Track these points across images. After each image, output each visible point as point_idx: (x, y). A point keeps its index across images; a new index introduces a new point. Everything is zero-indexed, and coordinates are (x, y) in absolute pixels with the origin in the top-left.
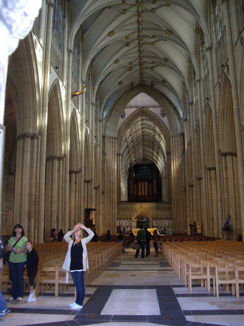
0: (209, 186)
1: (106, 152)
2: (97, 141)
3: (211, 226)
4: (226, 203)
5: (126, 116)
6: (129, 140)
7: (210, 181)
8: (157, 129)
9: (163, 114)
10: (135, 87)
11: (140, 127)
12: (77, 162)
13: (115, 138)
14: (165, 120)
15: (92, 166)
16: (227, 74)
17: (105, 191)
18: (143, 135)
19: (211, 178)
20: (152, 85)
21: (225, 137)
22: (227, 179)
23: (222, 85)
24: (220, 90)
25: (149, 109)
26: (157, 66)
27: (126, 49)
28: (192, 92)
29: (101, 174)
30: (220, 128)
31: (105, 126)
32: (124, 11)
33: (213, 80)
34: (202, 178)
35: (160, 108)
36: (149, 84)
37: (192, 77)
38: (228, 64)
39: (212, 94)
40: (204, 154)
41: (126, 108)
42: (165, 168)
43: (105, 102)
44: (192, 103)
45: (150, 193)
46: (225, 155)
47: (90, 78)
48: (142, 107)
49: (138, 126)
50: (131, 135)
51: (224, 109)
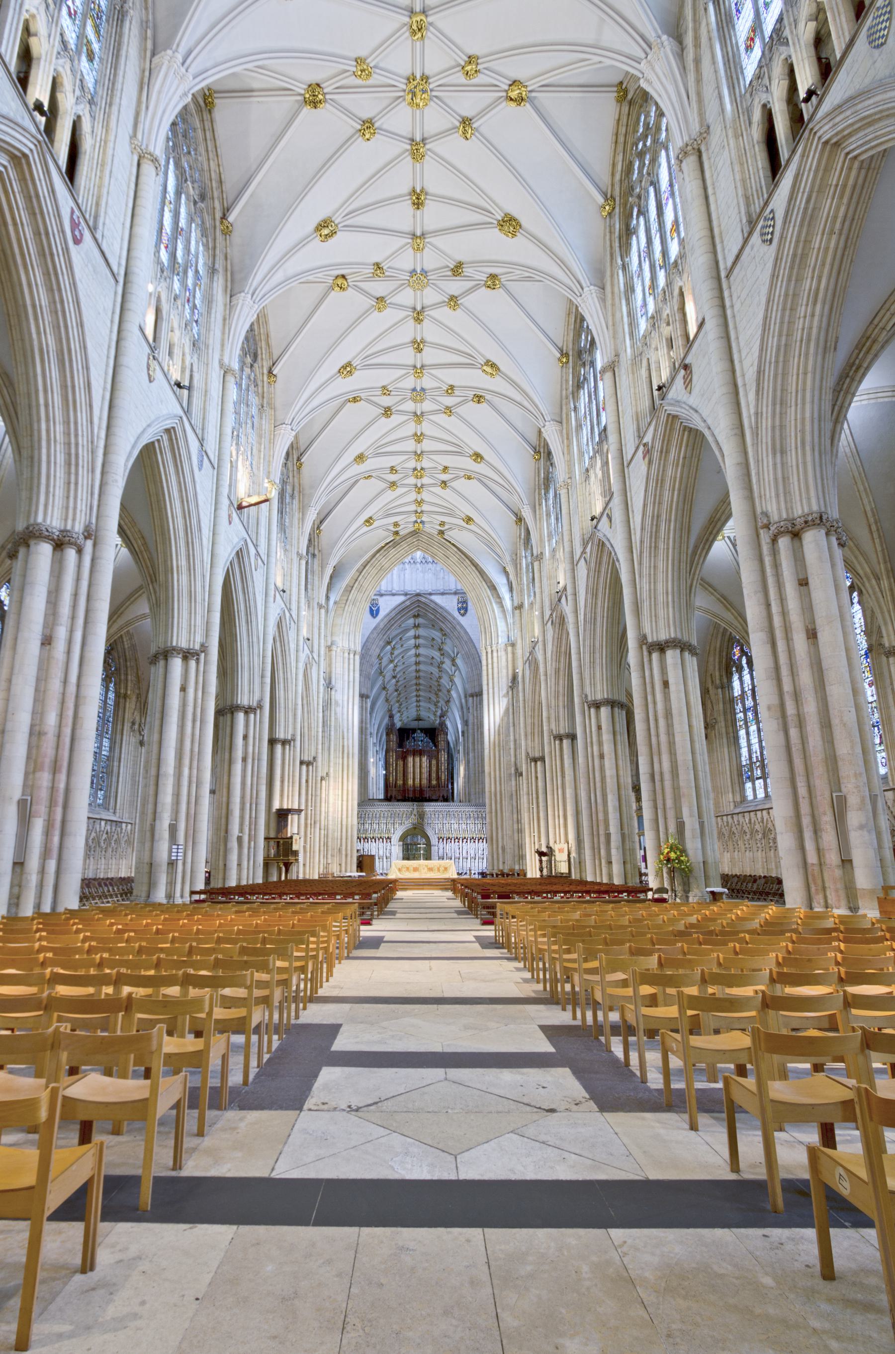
0: (595, 748)
1: (333, 682)
2: (312, 652)
4: (668, 784)
10: (405, 538)
11: (412, 642)
15: (296, 704)
18: (417, 663)
19: (599, 728)
20: (441, 533)
21: (661, 598)
22: (668, 714)
23: (658, 445)
25: (433, 598)
27: (385, 424)
28: (541, 530)
29: (320, 730)
30: (645, 571)
35: (457, 597)
37: (540, 494)
42: (463, 732)
43: (333, 562)
45: (434, 782)
46: (661, 647)
48: (418, 595)
49: (409, 639)
51: (658, 516)
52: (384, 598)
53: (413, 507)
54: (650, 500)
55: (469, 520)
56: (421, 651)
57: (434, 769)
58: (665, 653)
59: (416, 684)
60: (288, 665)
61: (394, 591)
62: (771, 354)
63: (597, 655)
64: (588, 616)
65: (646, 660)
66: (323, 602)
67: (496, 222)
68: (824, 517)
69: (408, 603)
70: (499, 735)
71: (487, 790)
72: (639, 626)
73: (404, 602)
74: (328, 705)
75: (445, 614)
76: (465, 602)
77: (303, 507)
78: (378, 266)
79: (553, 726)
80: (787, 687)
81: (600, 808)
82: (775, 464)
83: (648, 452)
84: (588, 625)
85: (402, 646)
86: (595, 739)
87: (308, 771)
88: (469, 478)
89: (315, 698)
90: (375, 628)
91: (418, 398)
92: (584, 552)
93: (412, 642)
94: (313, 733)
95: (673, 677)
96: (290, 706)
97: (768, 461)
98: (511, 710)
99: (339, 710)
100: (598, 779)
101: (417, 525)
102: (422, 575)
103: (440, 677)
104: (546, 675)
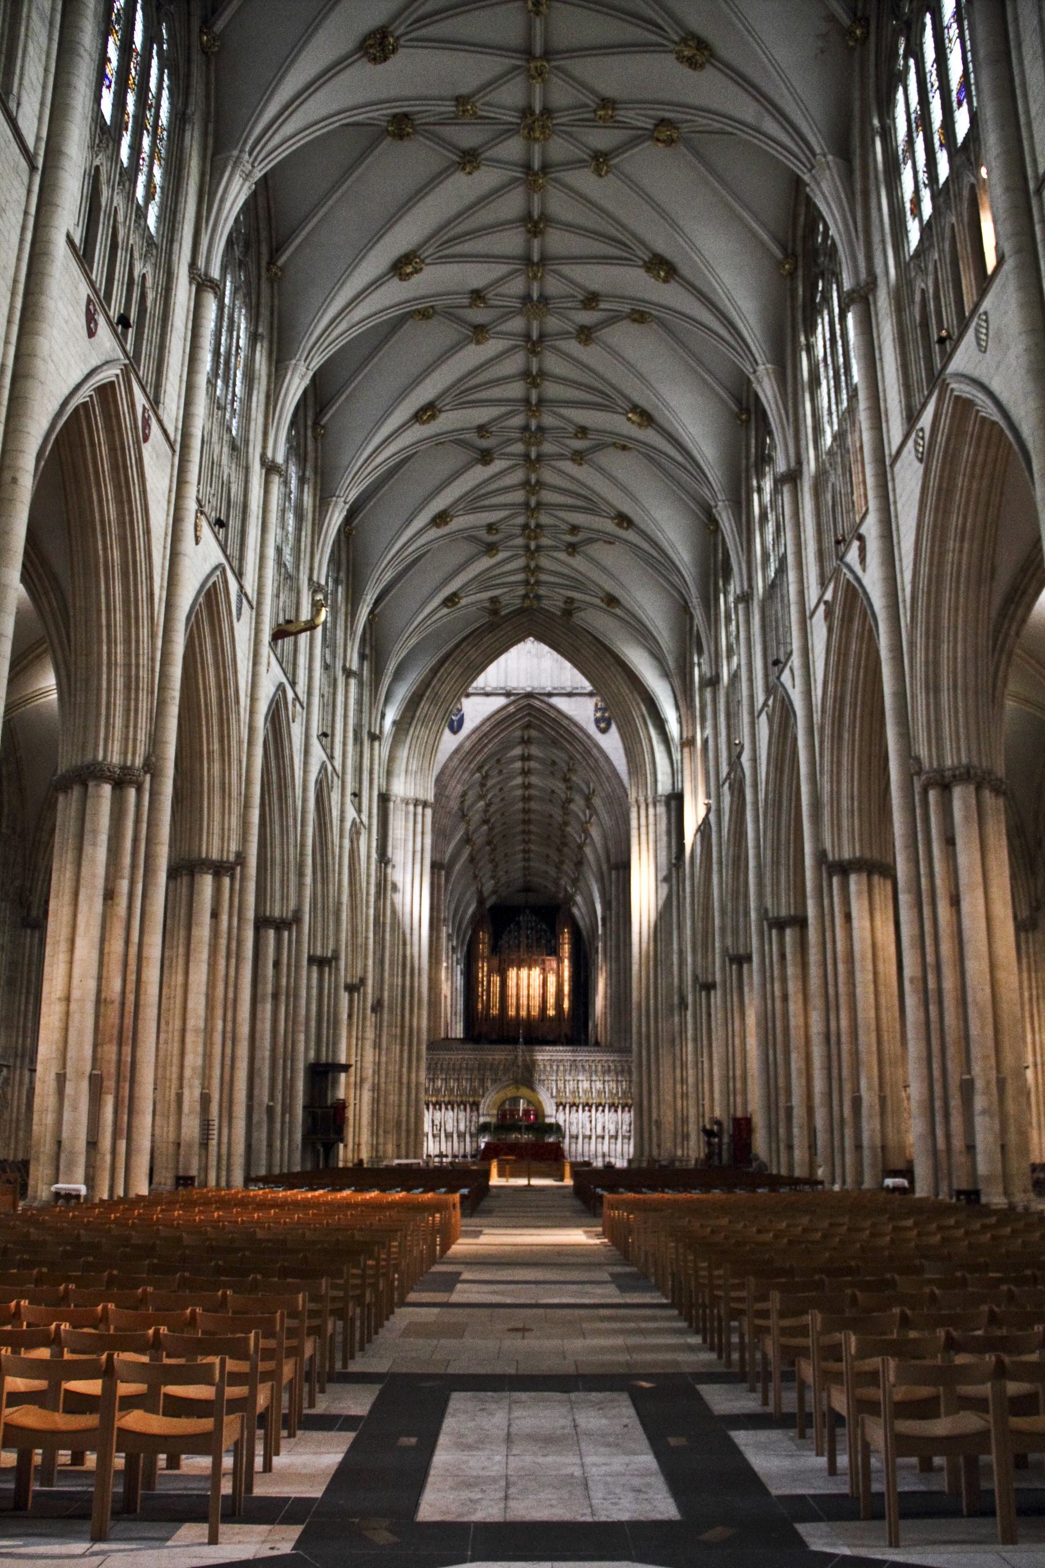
1: (390, 854)
2: (359, 811)
5: (468, 726)
6: (476, 817)
9: (603, 724)
11: (518, 765)
13: (425, 805)
14: (611, 743)
15: (339, 903)
16: (857, 568)
17: (386, 1003)
18: (526, 799)
19: (783, 956)
20: (568, 613)
21: (845, 803)
23: (838, 612)
24: (830, 630)
25: (555, 701)
26: (590, 541)
27: (479, 473)
29: (371, 935)
31: (391, 759)
32: (479, 332)
33: (801, 593)
34: (749, 959)
35: (594, 700)
37: (716, 584)
38: (863, 530)
39: (796, 645)
40: (759, 866)
41: (468, 695)
42: (604, 919)
44: (713, 682)
45: (551, 1012)
46: (843, 869)
47: (342, 575)
48: (529, 695)
49: (513, 760)
50: (481, 797)
52: (472, 699)
53: (520, 577)
54: (831, 676)
55: (612, 600)
56: (534, 780)
57: (552, 989)
59: (524, 832)
61: (488, 689)
62: (923, 584)
63: (783, 853)
64: (770, 796)
67: (641, 263)
68: (972, 772)
69: (512, 709)
70: (655, 941)
71: (634, 1029)
72: (817, 838)
74: (384, 887)
78: (477, 296)
79: (729, 941)
80: (930, 959)
81: (781, 1071)
82: (928, 705)
83: (829, 615)
84: (770, 811)
85: (500, 772)
86: (776, 973)
88: (610, 543)
89: (364, 885)
90: (456, 751)
91: (533, 440)
92: (765, 704)
93: (518, 765)
95: (860, 907)
97: (921, 699)
98: (675, 903)
99: (398, 898)
100: (779, 1031)
101: (527, 603)
102: (535, 661)
103: (566, 824)
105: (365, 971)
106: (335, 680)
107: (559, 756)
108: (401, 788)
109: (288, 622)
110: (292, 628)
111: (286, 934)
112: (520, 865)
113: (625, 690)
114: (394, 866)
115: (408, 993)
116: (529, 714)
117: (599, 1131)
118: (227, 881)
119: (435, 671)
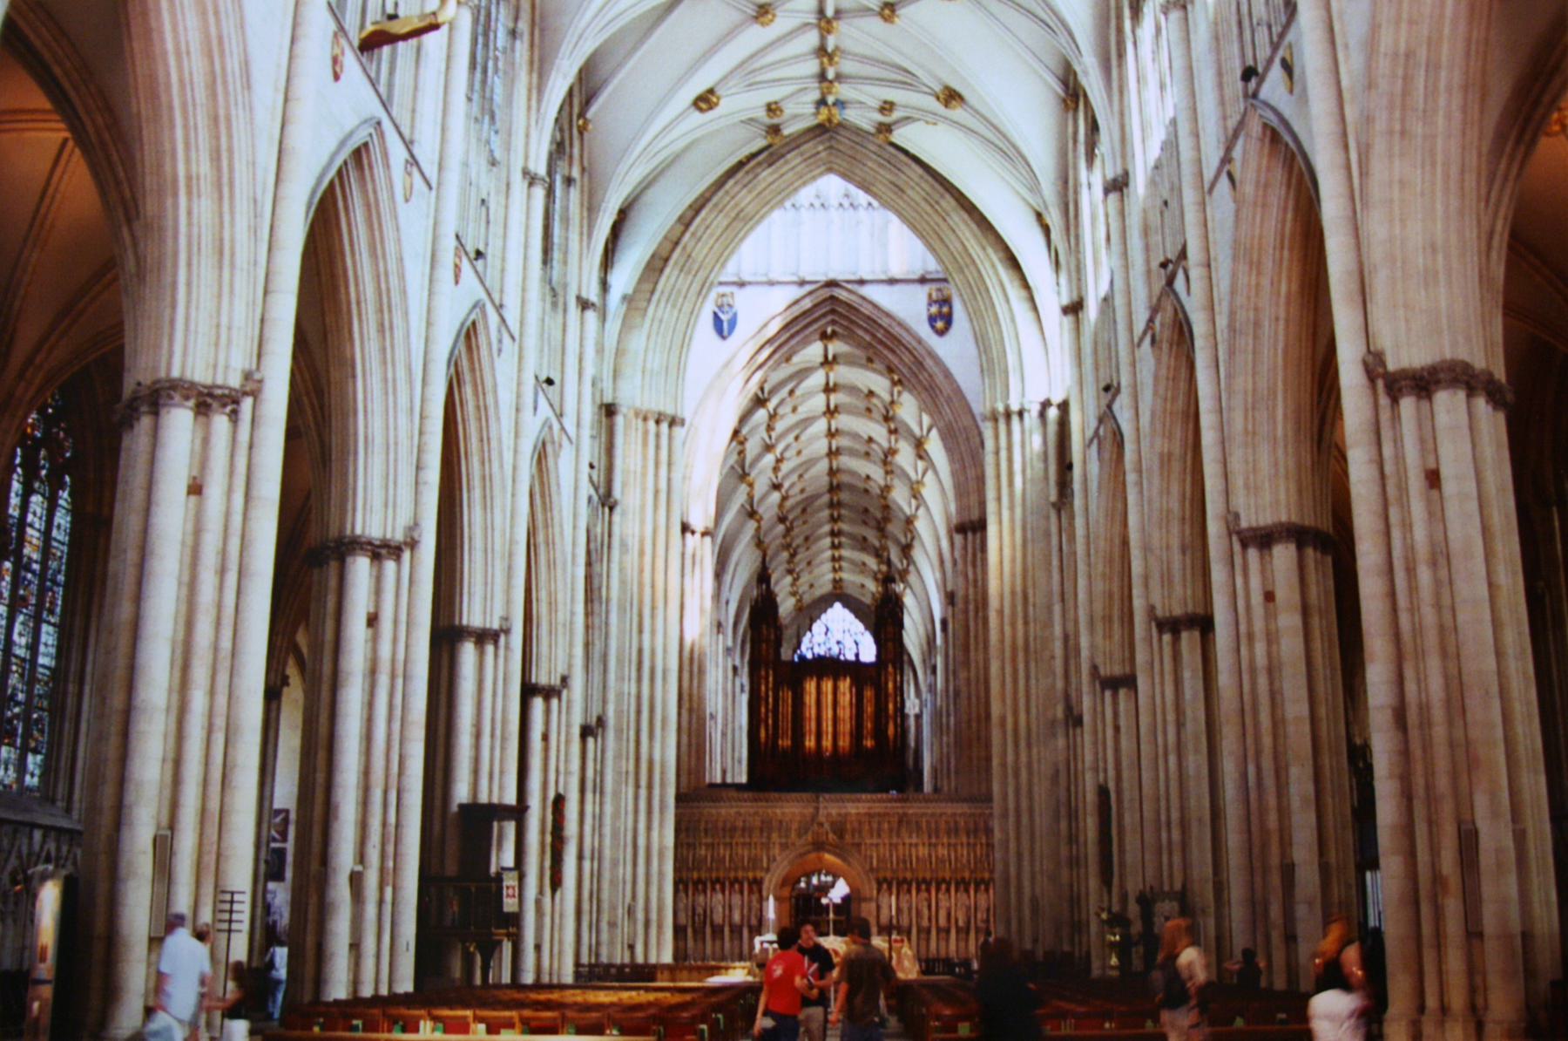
1: (617, 493)
3: (1275, 911)
6: (762, 482)
7: (1270, 616)
8: (908, 409)
10: (797, 141)
11: (819, 402)
12: (390, 479)
15: (512, 542)
18: (832, 453)
20: (885, 129)
25: (868, 291)
31: (619, 353)
35: (926, 289)
36: (863, 118)
37: (1120, 30)
42: (944, 623)
45: (869, 743)
46: (1423, 383)
47: (523, 26)
48: (832, 284)
49: (809, 394)
52: (748, 290)
55: (951, 97)
56: (843, 421)
57: (869, 709)
58: (1429, 397)
60: (494, 444)
65: (1385, 416)
66: (593, 294)
69: (807, 304)
73: (796, 302)
75: (896, 330)
76: (946, 301)
77: (542, 60)
85: (794, 410)
87: (548, 712)
93: (821, 398)
94: (561, 616)
96: (498, 547)
98: (1055, 562)
101: (824, 111)
103: (887, 488)
104: (1140, 471)
105: (570, 666)
106: (508, 185)
107: (879, 383)
108: (633, 394)
109: (393, 17)
110: (397, 28)
111: (390, 566)
112: (829, 553)
113: (974, 247)
114: (624, 514)
115: (644, 709)
116: (833, 311)
117: (942, 922)
118: (221, 422)
119: (686, 221)
